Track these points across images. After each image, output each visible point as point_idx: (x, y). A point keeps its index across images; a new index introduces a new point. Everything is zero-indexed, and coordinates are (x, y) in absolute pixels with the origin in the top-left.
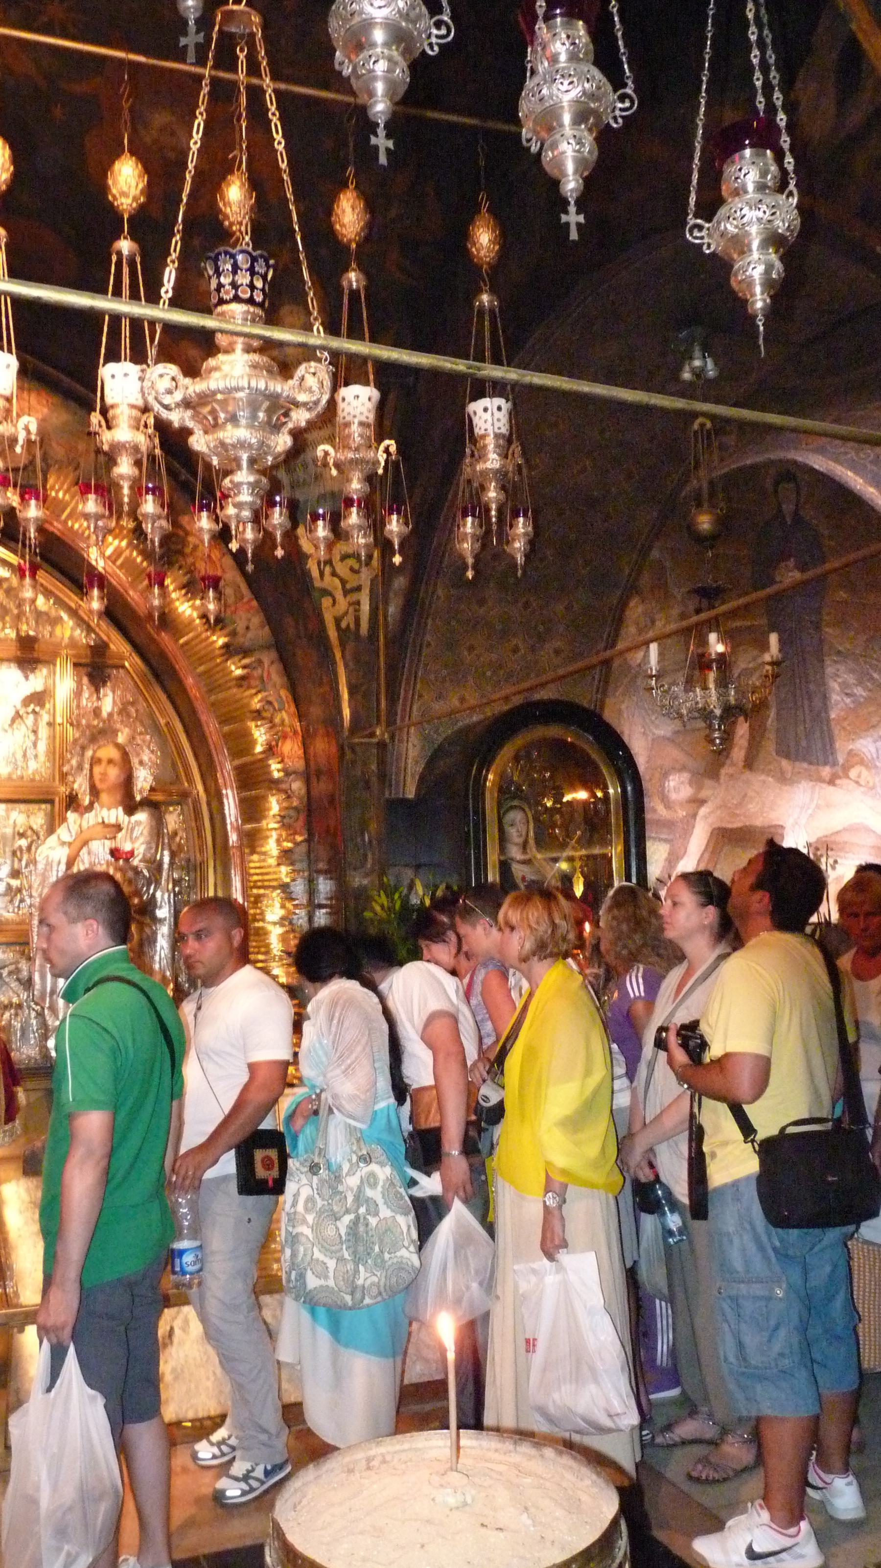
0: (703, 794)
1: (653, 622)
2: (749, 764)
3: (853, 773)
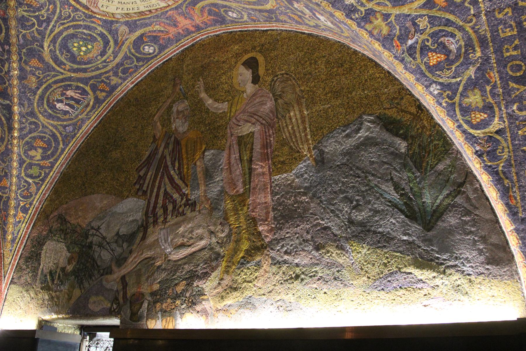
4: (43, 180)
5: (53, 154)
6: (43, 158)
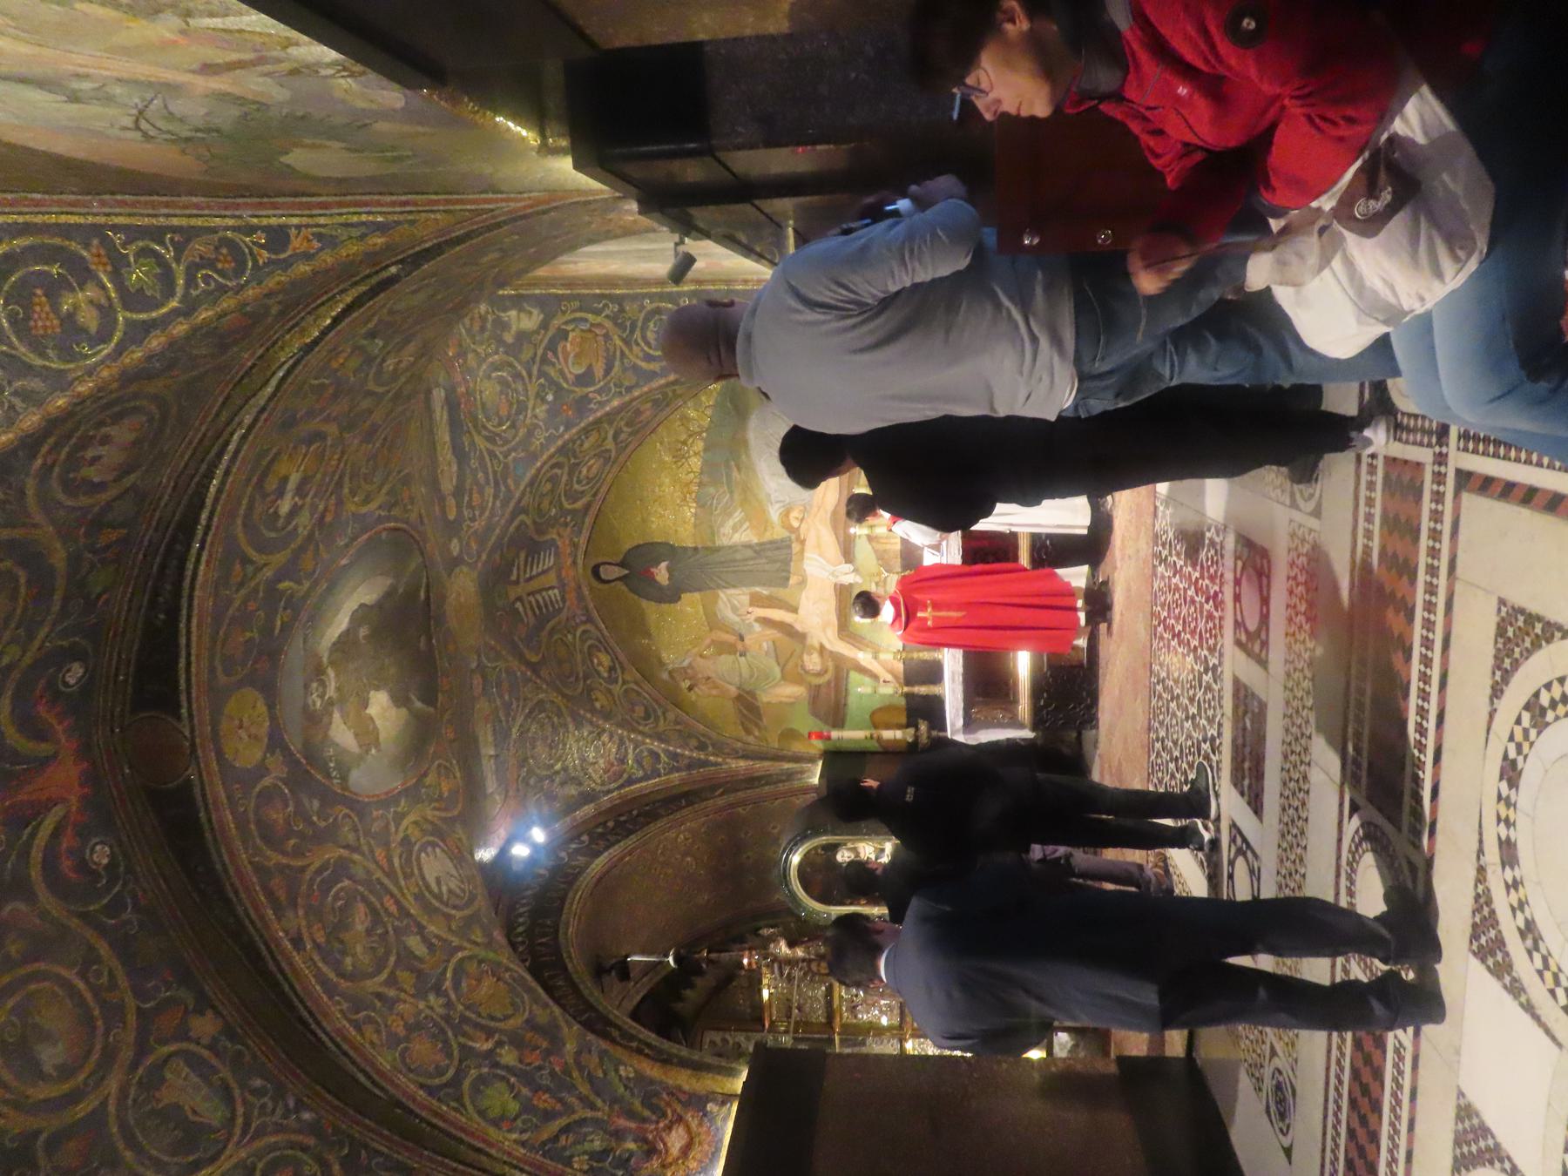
0: (817, 645)
1: (709, 678)
2: (795, 610)
3: (795, 524)
4: (157, 234)
5: (52, 255)
6: (84, 274)
